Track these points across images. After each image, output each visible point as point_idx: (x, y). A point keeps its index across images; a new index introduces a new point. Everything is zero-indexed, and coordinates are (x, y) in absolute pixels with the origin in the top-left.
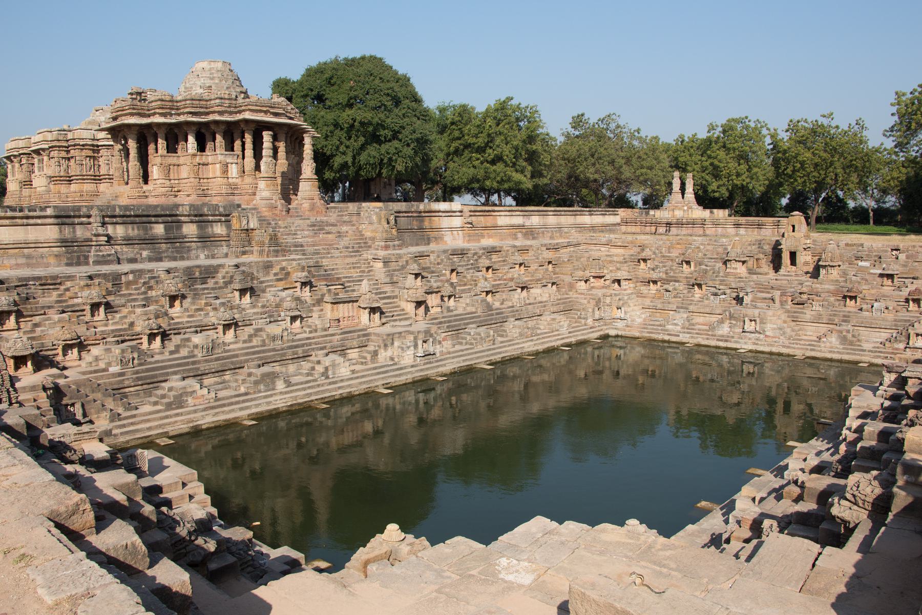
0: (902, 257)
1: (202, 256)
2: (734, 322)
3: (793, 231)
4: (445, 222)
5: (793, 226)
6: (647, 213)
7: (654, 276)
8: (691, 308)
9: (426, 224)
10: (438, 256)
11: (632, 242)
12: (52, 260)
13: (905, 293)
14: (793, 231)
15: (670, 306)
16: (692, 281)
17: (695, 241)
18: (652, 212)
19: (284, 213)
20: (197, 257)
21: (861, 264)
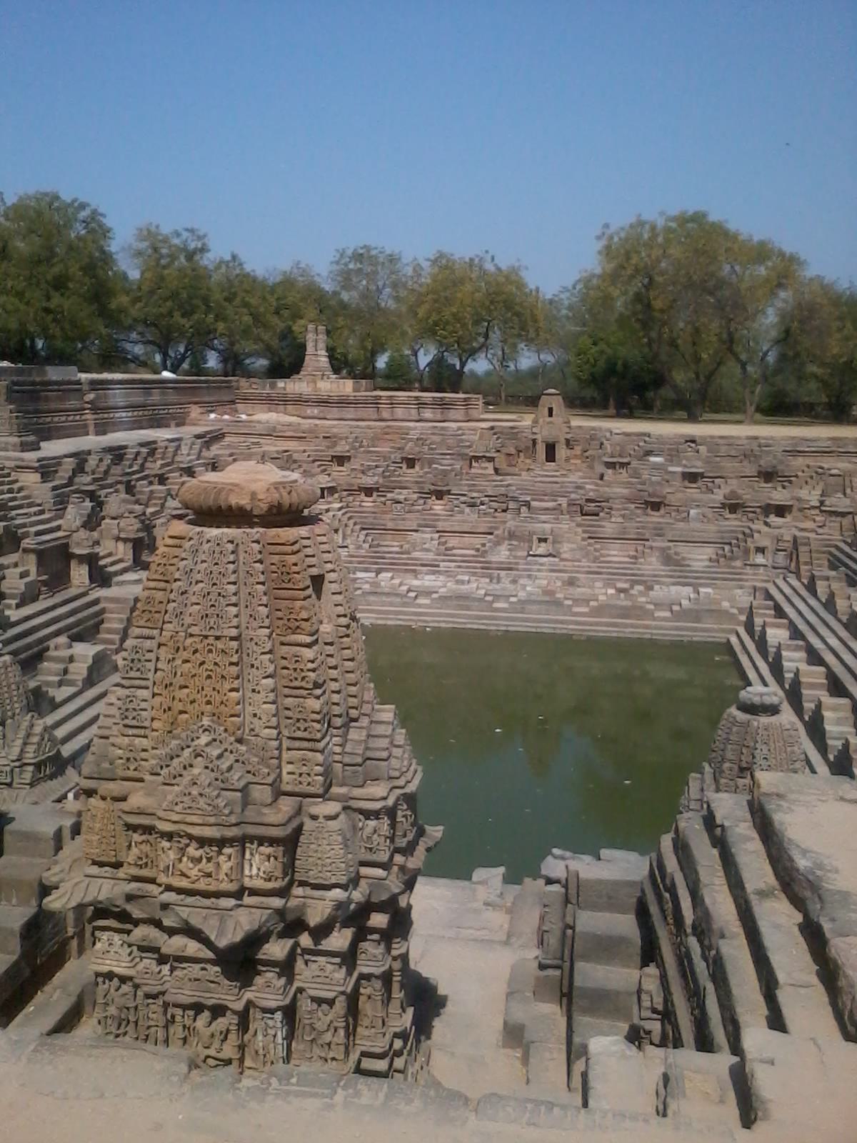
0: (702, 449)
2: (515, 543)
3: (551, 415)
5: (551, 410)
6: (273, 386)
7: (368, 481)
8: (441, 525)
10: (101, 460)
11: (310, 431)
13: (719, 496)
14: (551, 415)
15: (408, 523)
16: (428, 487)
17: (410, 429)
18: (281, 384)
21: (653, 459)
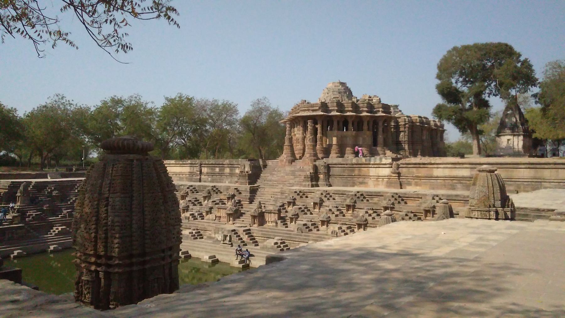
1: (227, 182)
4: (373, 172)
9: (356, 172)
12: (185, 179)
19: (287, 164)
20: (225, 182)
